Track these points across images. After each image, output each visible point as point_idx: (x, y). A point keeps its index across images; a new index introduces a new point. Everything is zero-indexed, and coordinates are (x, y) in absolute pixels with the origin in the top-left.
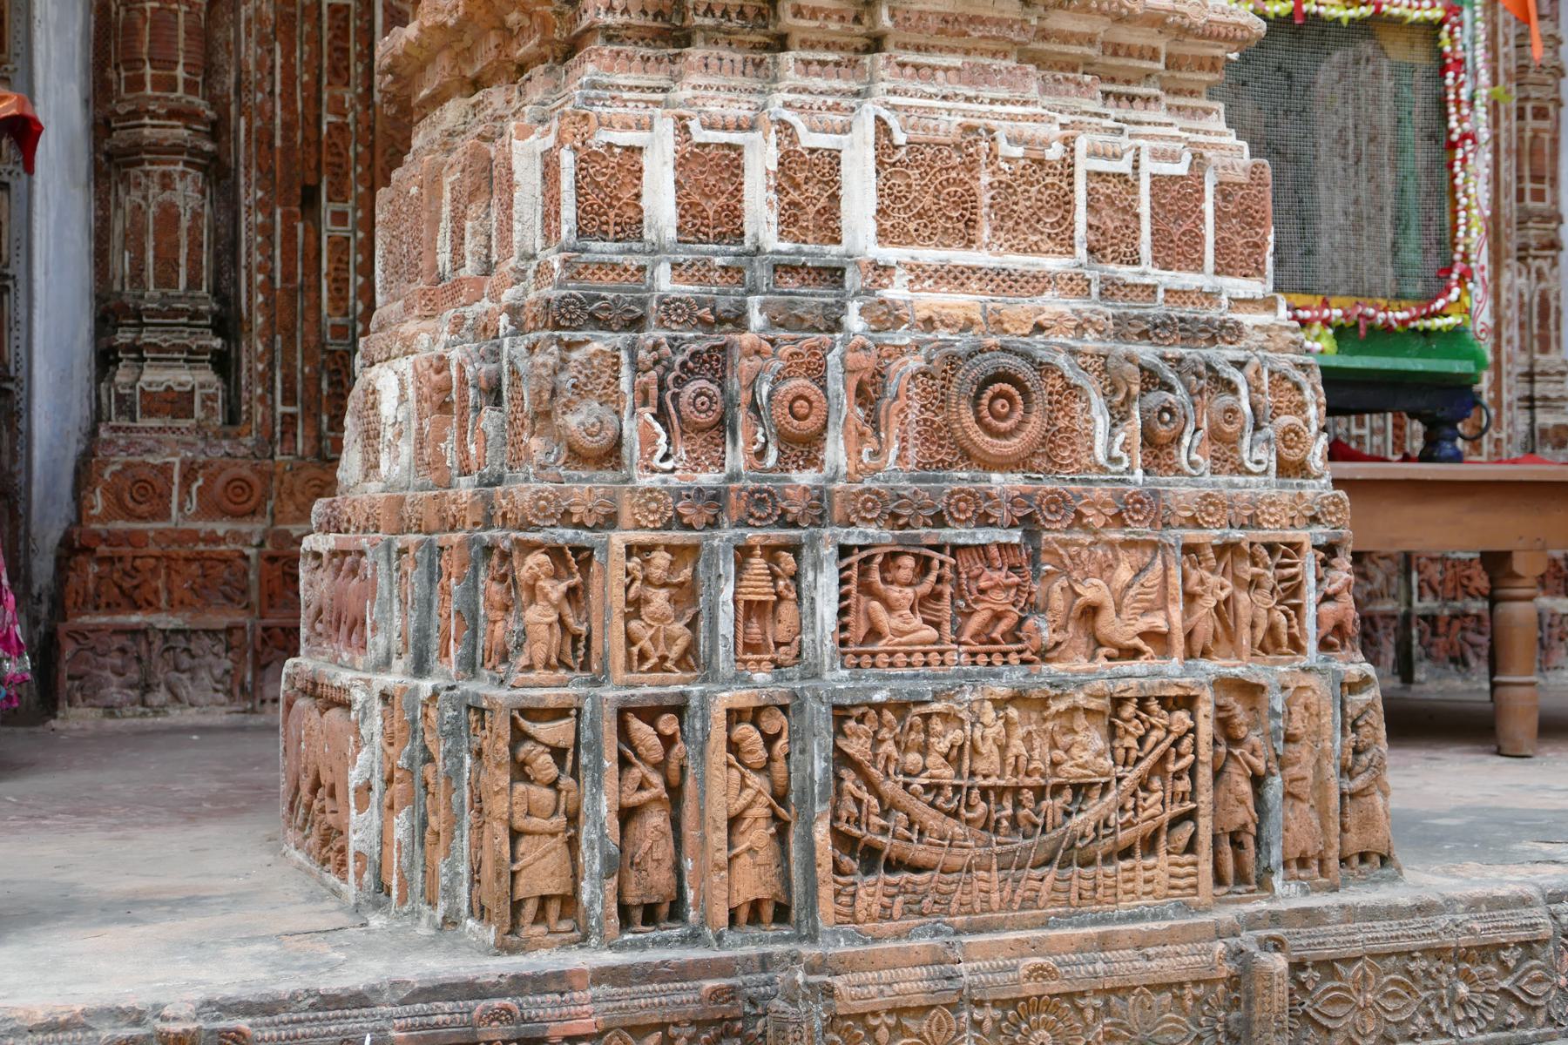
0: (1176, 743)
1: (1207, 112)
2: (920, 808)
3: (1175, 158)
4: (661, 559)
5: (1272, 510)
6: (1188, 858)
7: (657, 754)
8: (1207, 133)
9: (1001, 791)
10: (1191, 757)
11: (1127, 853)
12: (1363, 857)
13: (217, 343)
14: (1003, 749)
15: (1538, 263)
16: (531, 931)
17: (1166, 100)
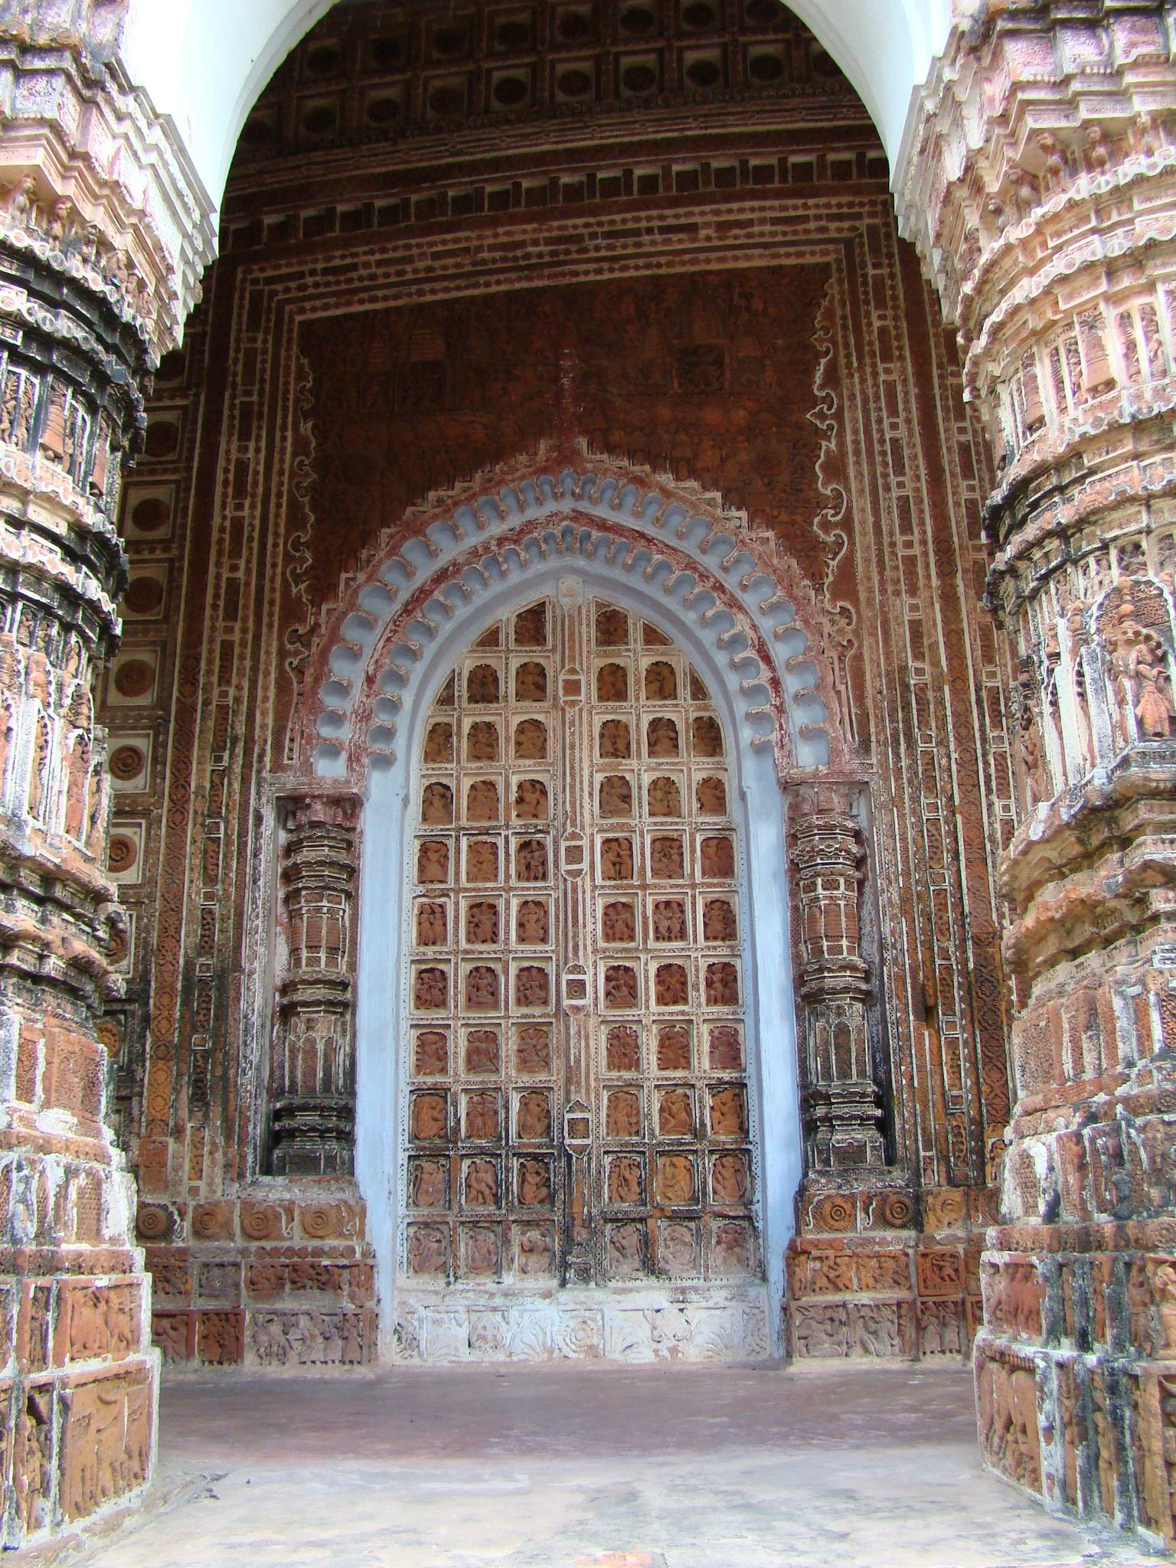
13: (879, 1112)
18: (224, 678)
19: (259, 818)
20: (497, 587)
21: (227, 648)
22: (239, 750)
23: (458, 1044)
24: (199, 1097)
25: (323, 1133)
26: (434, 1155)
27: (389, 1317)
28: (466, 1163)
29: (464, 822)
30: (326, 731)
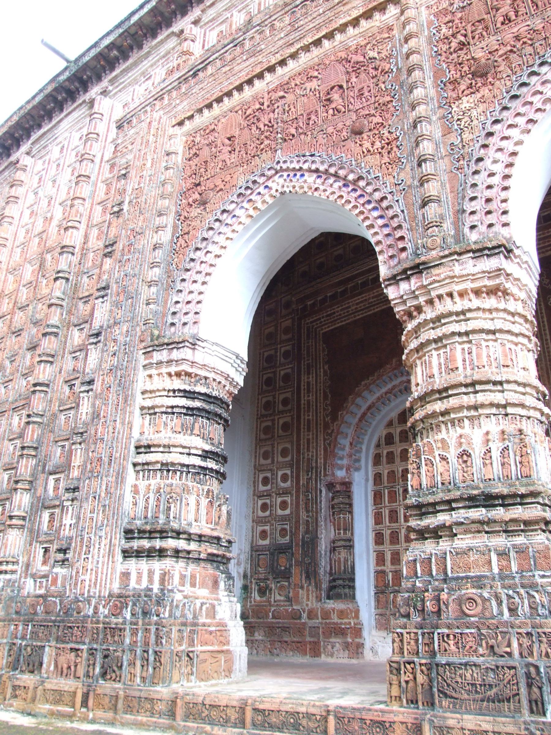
2: (454, 685)
4: (412, 635)
7: (411, 670)
9: (472, 684)
11: (503, 701)
14: (472, 675)
16: (393, 702)
18: (308, 450)
19: (321, 491)
20: (387, 408)
21: (308, 440)
22: (314, 471)
23: (388, 557)
24: (308, 577)
25: (344, 587)
26: (383, 592)
27: (368, 644)
28: (392, 595)
29: (386, 484)
30: (339, 462)
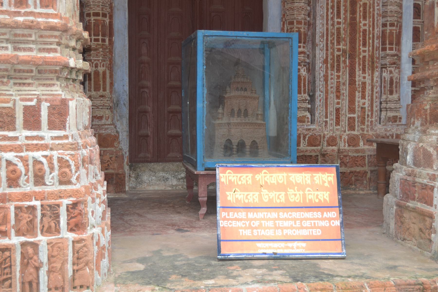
0: (5, 260)
1: (54, 85)
3: (31, 100)
5: (52, 195)
6: (10, 289)
8: (51, 91)
10: (9, 264)
12: (81, 287)
15: (390, 69)
17: (37, 82)
